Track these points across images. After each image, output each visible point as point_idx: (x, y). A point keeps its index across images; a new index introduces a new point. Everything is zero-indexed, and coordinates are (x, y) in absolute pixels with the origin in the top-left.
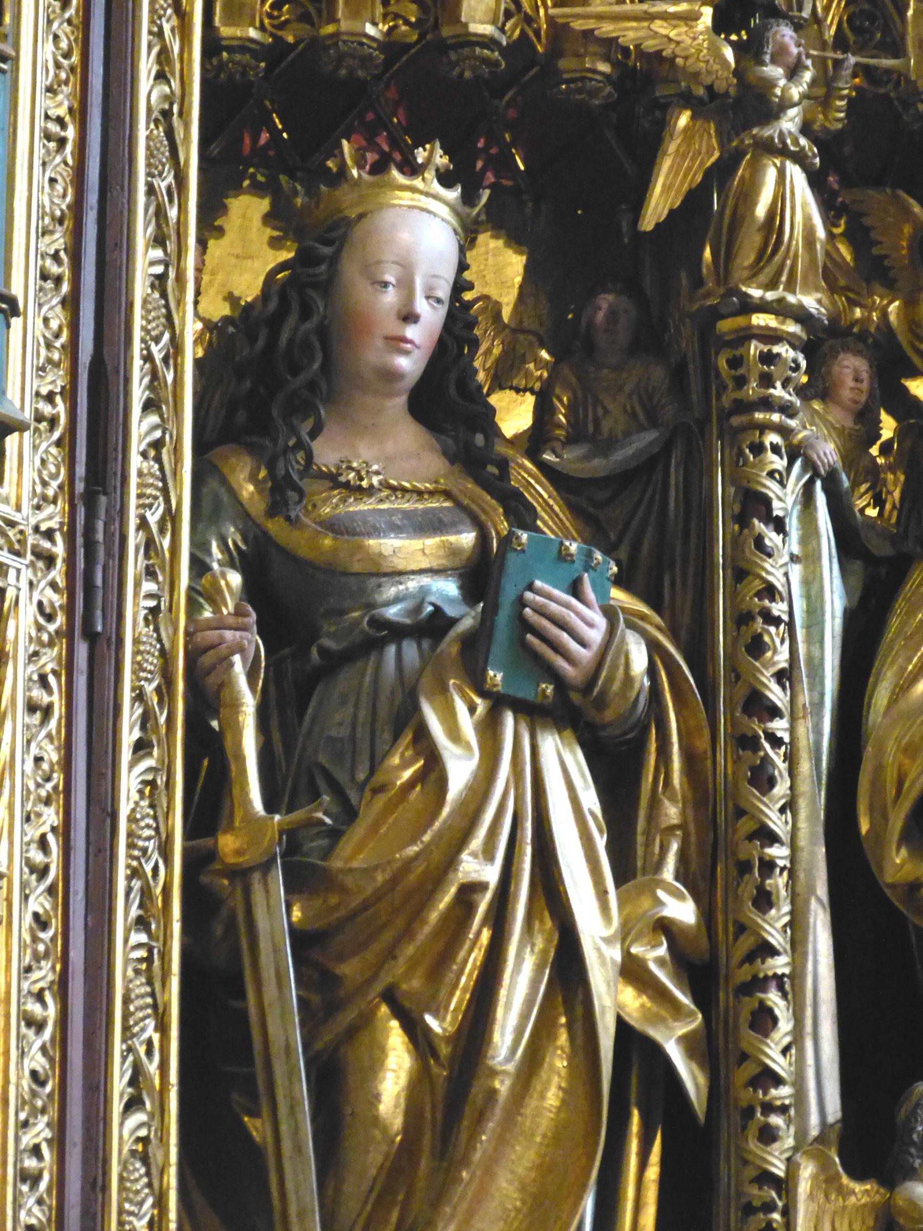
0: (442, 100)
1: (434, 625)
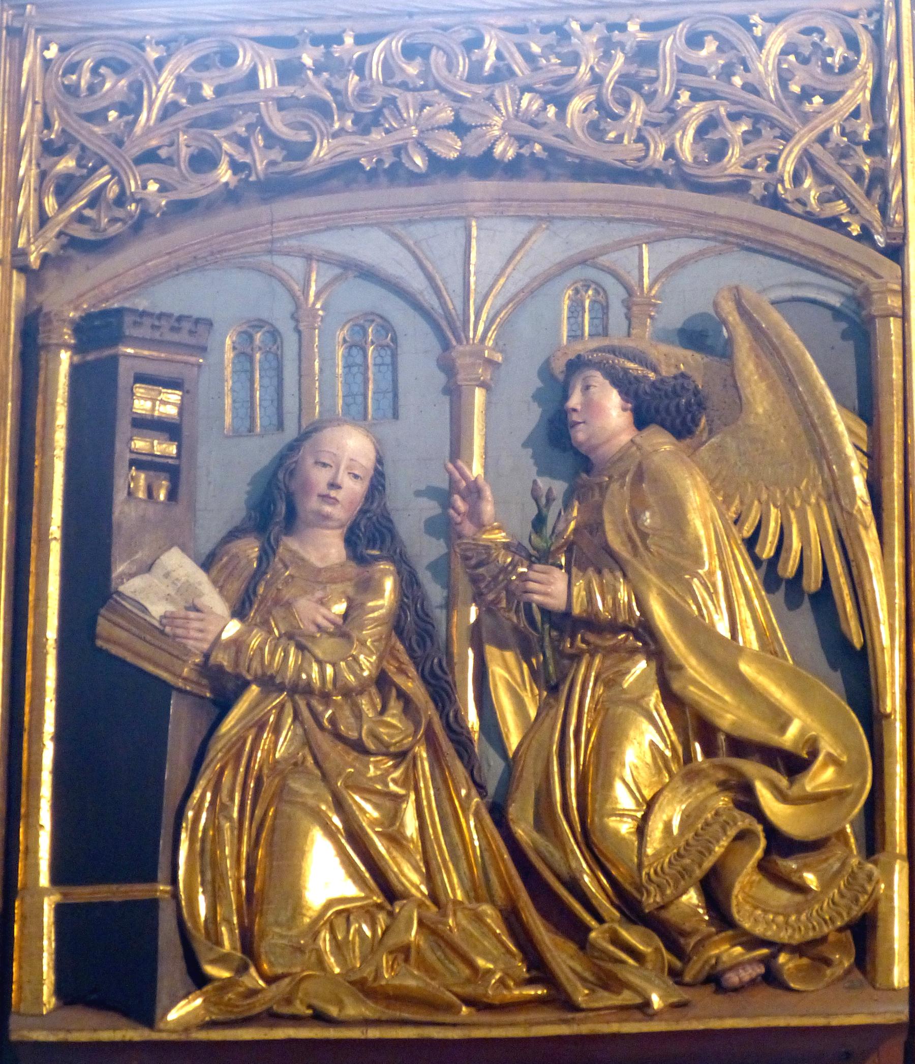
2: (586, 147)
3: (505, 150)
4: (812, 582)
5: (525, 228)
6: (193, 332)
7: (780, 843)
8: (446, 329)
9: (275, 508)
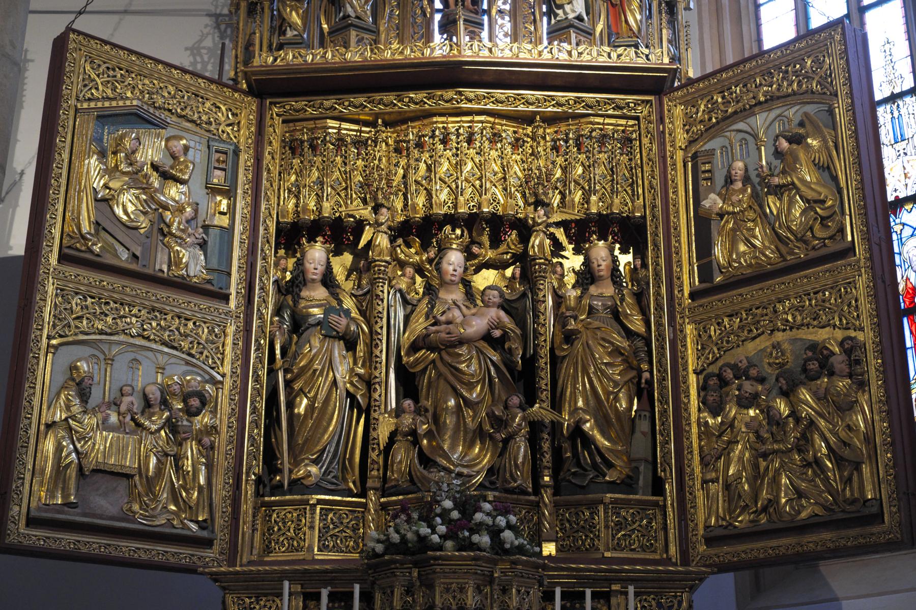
0: (315, 229)
1: (319, 323)
2: (778, 94)
3: (762, 99)
4: (826, 165)
5: (767, 113)
6: (711, 153)
7: (823, 218)
8: (755, 136)
9: (729, 180)
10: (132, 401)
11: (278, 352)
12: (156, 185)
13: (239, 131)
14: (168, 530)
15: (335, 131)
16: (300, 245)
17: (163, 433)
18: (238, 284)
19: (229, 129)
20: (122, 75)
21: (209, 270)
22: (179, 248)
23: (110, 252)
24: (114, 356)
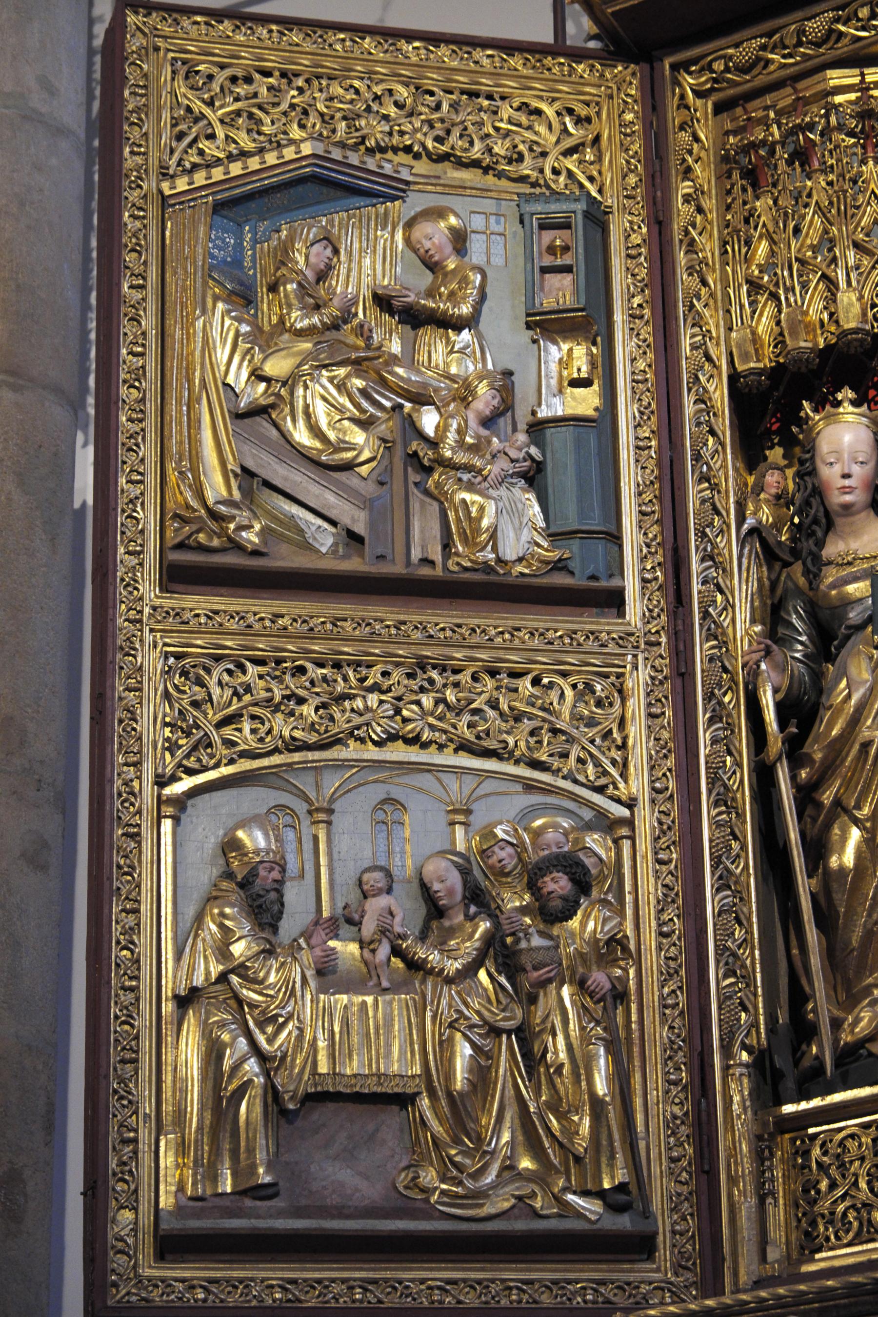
10: (405, 911)
11: (770, 715)
12: (396, 347)
13: (599, 159)
14: (521, 1225)
15: (853, 96)
16: (801, 422)
17: (482, 975)
18: (644, 559)
19: (570, 163)
20: (270, 88)
21: (555, 536)
22: (468, 496)
23: (289, 541)
24: (332, 800)
